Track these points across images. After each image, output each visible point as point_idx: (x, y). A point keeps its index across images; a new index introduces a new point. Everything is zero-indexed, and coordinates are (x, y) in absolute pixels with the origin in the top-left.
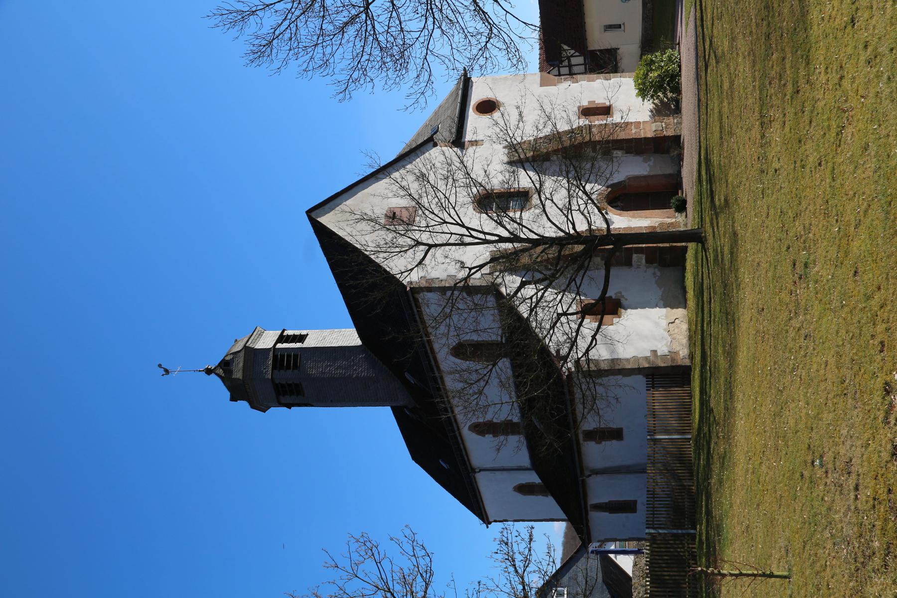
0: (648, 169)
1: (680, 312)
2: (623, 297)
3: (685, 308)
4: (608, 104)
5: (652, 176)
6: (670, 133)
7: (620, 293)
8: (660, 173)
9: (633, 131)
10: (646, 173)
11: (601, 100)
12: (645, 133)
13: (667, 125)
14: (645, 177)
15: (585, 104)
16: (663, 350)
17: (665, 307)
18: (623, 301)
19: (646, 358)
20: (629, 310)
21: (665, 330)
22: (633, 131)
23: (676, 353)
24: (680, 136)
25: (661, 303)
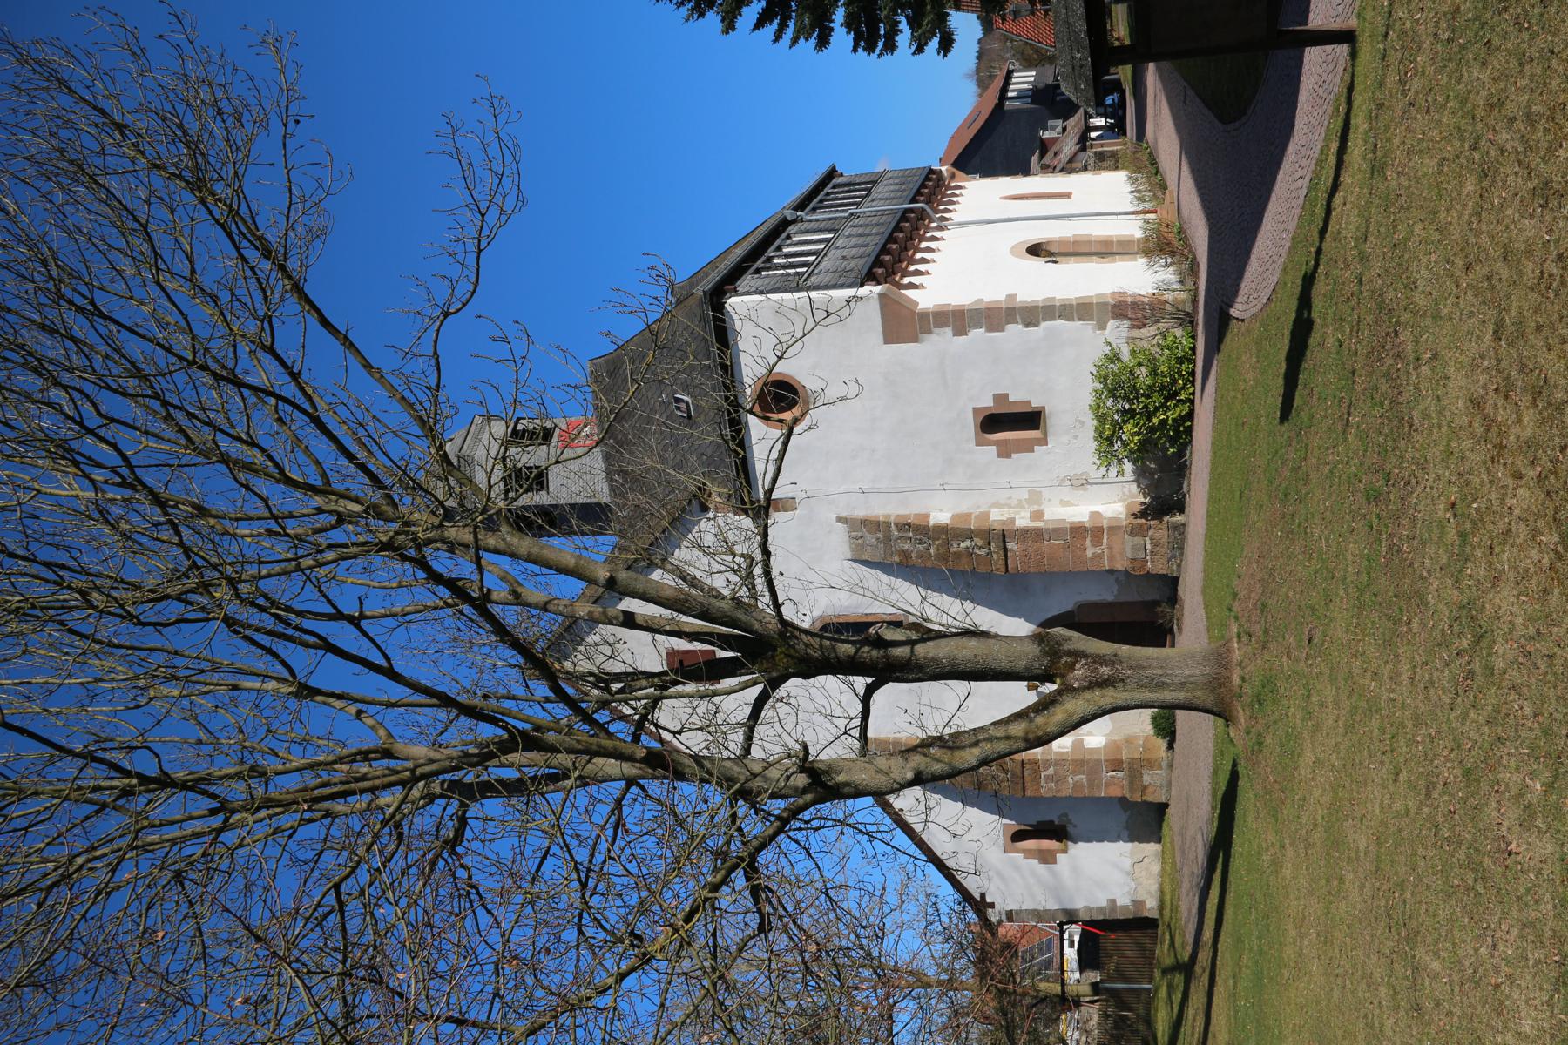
0: (1115, 588)
1: (1152, 848)
2: (1070, 821)
3: (1159, 841)
4: (1036, 404)
5: (1121, 604)
6: (1157, 566)
7: (1066, 815)
8: (1137, 598)
9: (1089, 553)
10: (1110, 598)
11: (1022, 394)
12: (1111, 559)
13: (1155, 544)
14: (1110, 605)
15: (987, 402)
16: (1123, 900)
17: (1131, 841)
18: (1070, 829)
19: (1101, 909)
20: (1081, 844)
21: (1128, 873)
22: (1089, 553)
23: (1142, 903)
24: (1177, 579)
25: (1126, 833)
